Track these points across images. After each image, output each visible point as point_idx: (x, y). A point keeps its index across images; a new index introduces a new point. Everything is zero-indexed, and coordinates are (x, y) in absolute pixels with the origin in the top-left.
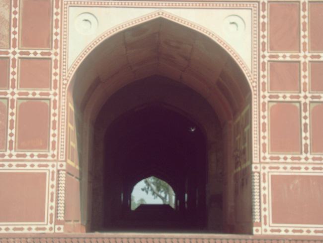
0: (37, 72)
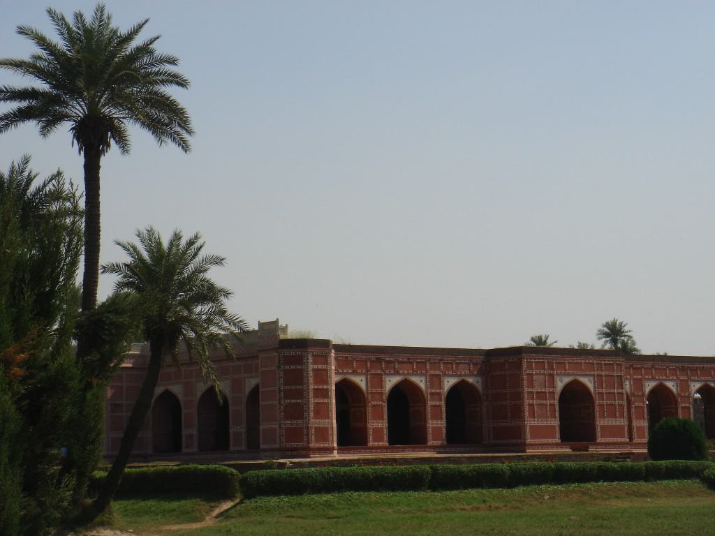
0: (553, 393)
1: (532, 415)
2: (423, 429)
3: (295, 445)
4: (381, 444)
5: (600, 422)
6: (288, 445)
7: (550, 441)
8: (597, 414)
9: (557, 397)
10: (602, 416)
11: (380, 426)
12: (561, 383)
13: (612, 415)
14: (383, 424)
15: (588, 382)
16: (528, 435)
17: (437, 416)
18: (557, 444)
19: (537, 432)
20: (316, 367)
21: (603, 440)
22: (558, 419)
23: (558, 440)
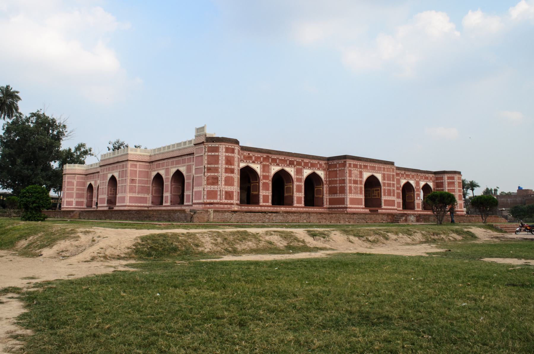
0: (361, 182)
1: (350, 193)
2: (292, 197)
3: (212, 201)
4: (267, 204)
5: (384, 198)
6: (208, 201)
7: (359, 206)
8: (382, 194)
9: (364, 183)
10: (385, 195)
11: (267, 194)
12: (366, 175)
13: (389, 195)
14: (269, 193)
15: (379, 176)
16: (348, 203)
17: (299, 191)
18: (363, 208)
19: (353, 201)
20: (227, 154)
21: (385, 207)
22: (363, 195)
23: (364, 207)
